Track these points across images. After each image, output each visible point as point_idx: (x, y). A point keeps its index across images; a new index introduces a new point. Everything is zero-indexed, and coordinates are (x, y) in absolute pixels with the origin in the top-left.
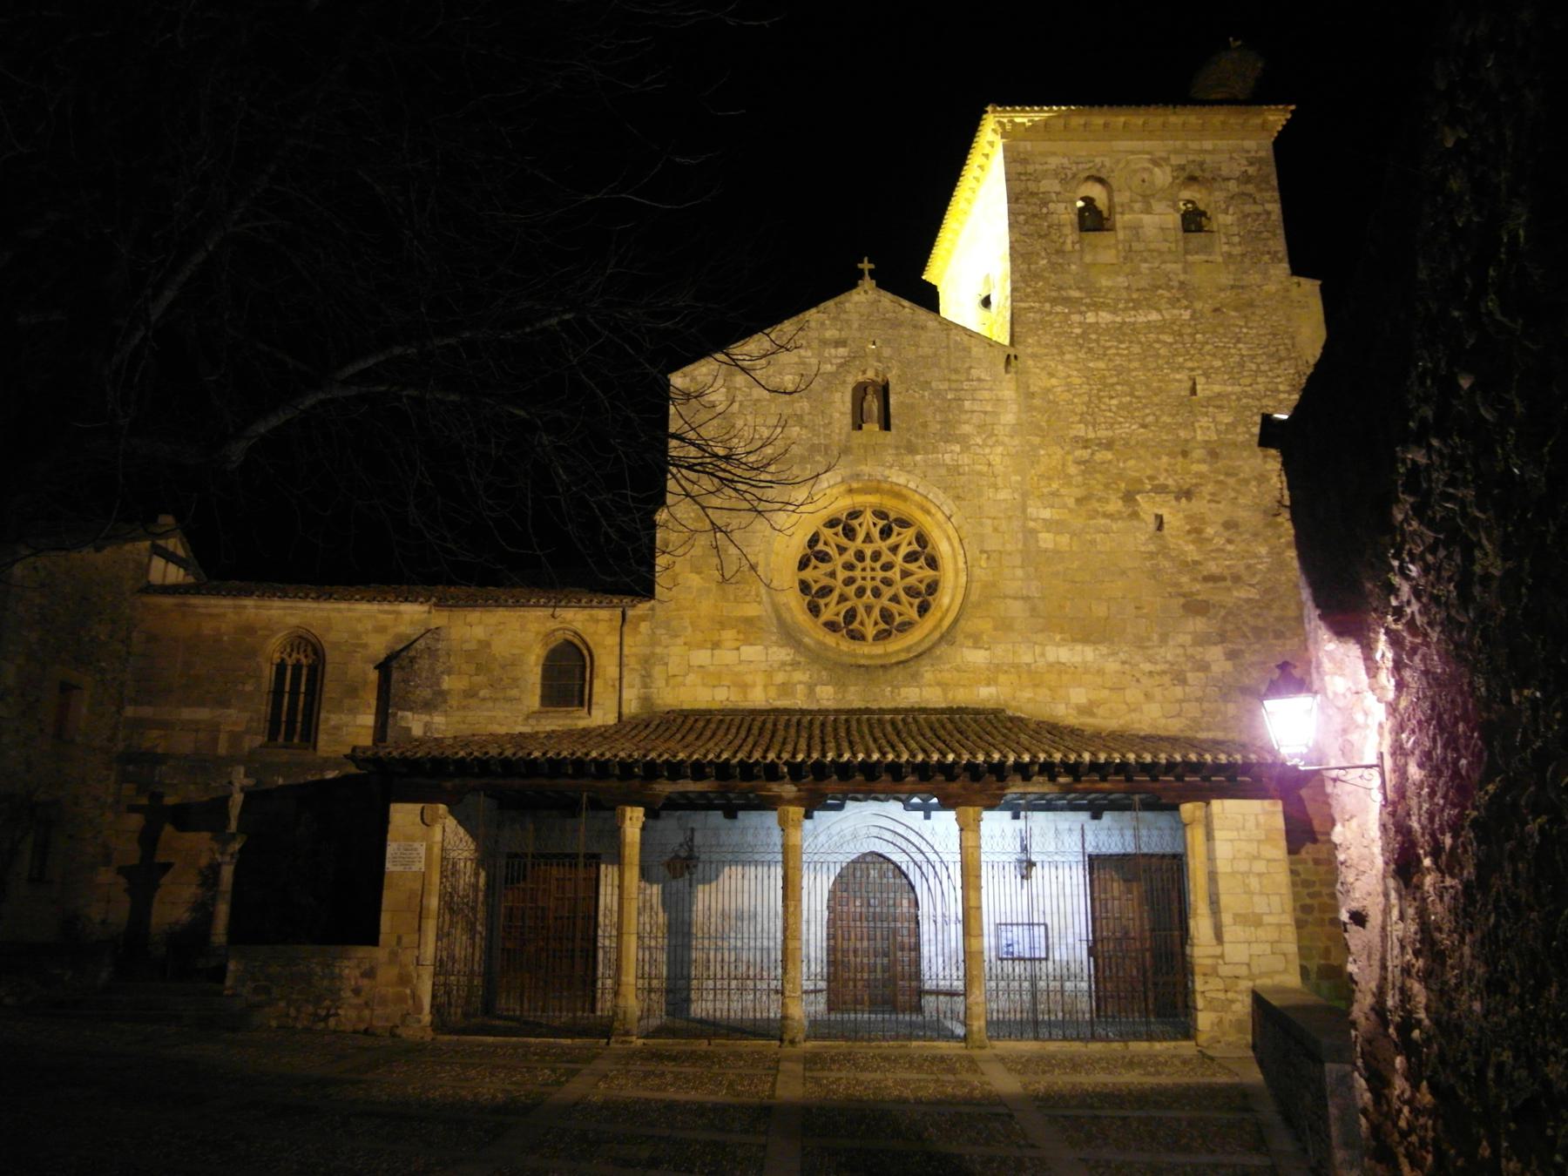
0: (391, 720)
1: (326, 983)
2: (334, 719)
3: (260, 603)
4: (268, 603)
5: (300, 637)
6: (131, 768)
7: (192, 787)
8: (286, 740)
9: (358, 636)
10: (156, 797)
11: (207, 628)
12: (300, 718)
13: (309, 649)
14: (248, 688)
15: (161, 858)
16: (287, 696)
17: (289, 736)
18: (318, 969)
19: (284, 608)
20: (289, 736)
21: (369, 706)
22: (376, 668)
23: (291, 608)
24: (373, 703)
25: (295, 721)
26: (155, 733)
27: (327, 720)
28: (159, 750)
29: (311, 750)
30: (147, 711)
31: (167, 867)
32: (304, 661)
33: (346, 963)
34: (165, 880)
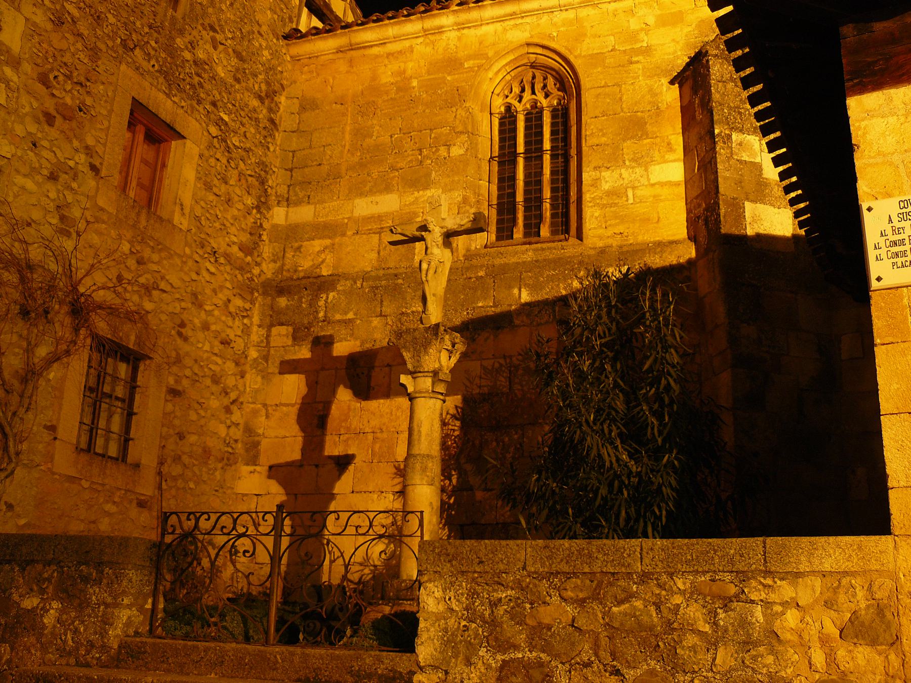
0: (721, 150)
1: (724, 657)
2: (609, 179)
3: (464, 16)
4: (474, 14)
5: (533, 66)
6: (283, 302)
7: (376, 322)
8: (527, 234)
9: (633, 37)
10: (323, 344)
11: (386, 76)
12: (547, 193)
13: (551, 81)
14: (456, 151)
15: (333, 447)
16: (521, 161)
17: (532, 230)
18: (694, 613)
19: (500, 20)
20: (532, 230)
21: (670, 148)
22: (672, 82)
23: (513, 15)
24: (678, 141)
25: (540, 200)
26: (317, 245)
27: (596, 183)
28: (325, 272)
29: (573, 240)
30: (304, 214)
31: (343, 462)
32: (544, 103)
33: (786, 590)
34: (343, 485)
